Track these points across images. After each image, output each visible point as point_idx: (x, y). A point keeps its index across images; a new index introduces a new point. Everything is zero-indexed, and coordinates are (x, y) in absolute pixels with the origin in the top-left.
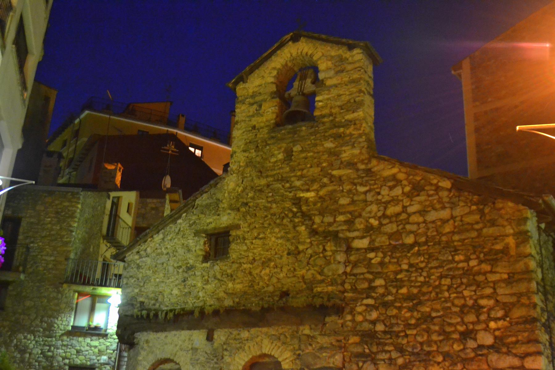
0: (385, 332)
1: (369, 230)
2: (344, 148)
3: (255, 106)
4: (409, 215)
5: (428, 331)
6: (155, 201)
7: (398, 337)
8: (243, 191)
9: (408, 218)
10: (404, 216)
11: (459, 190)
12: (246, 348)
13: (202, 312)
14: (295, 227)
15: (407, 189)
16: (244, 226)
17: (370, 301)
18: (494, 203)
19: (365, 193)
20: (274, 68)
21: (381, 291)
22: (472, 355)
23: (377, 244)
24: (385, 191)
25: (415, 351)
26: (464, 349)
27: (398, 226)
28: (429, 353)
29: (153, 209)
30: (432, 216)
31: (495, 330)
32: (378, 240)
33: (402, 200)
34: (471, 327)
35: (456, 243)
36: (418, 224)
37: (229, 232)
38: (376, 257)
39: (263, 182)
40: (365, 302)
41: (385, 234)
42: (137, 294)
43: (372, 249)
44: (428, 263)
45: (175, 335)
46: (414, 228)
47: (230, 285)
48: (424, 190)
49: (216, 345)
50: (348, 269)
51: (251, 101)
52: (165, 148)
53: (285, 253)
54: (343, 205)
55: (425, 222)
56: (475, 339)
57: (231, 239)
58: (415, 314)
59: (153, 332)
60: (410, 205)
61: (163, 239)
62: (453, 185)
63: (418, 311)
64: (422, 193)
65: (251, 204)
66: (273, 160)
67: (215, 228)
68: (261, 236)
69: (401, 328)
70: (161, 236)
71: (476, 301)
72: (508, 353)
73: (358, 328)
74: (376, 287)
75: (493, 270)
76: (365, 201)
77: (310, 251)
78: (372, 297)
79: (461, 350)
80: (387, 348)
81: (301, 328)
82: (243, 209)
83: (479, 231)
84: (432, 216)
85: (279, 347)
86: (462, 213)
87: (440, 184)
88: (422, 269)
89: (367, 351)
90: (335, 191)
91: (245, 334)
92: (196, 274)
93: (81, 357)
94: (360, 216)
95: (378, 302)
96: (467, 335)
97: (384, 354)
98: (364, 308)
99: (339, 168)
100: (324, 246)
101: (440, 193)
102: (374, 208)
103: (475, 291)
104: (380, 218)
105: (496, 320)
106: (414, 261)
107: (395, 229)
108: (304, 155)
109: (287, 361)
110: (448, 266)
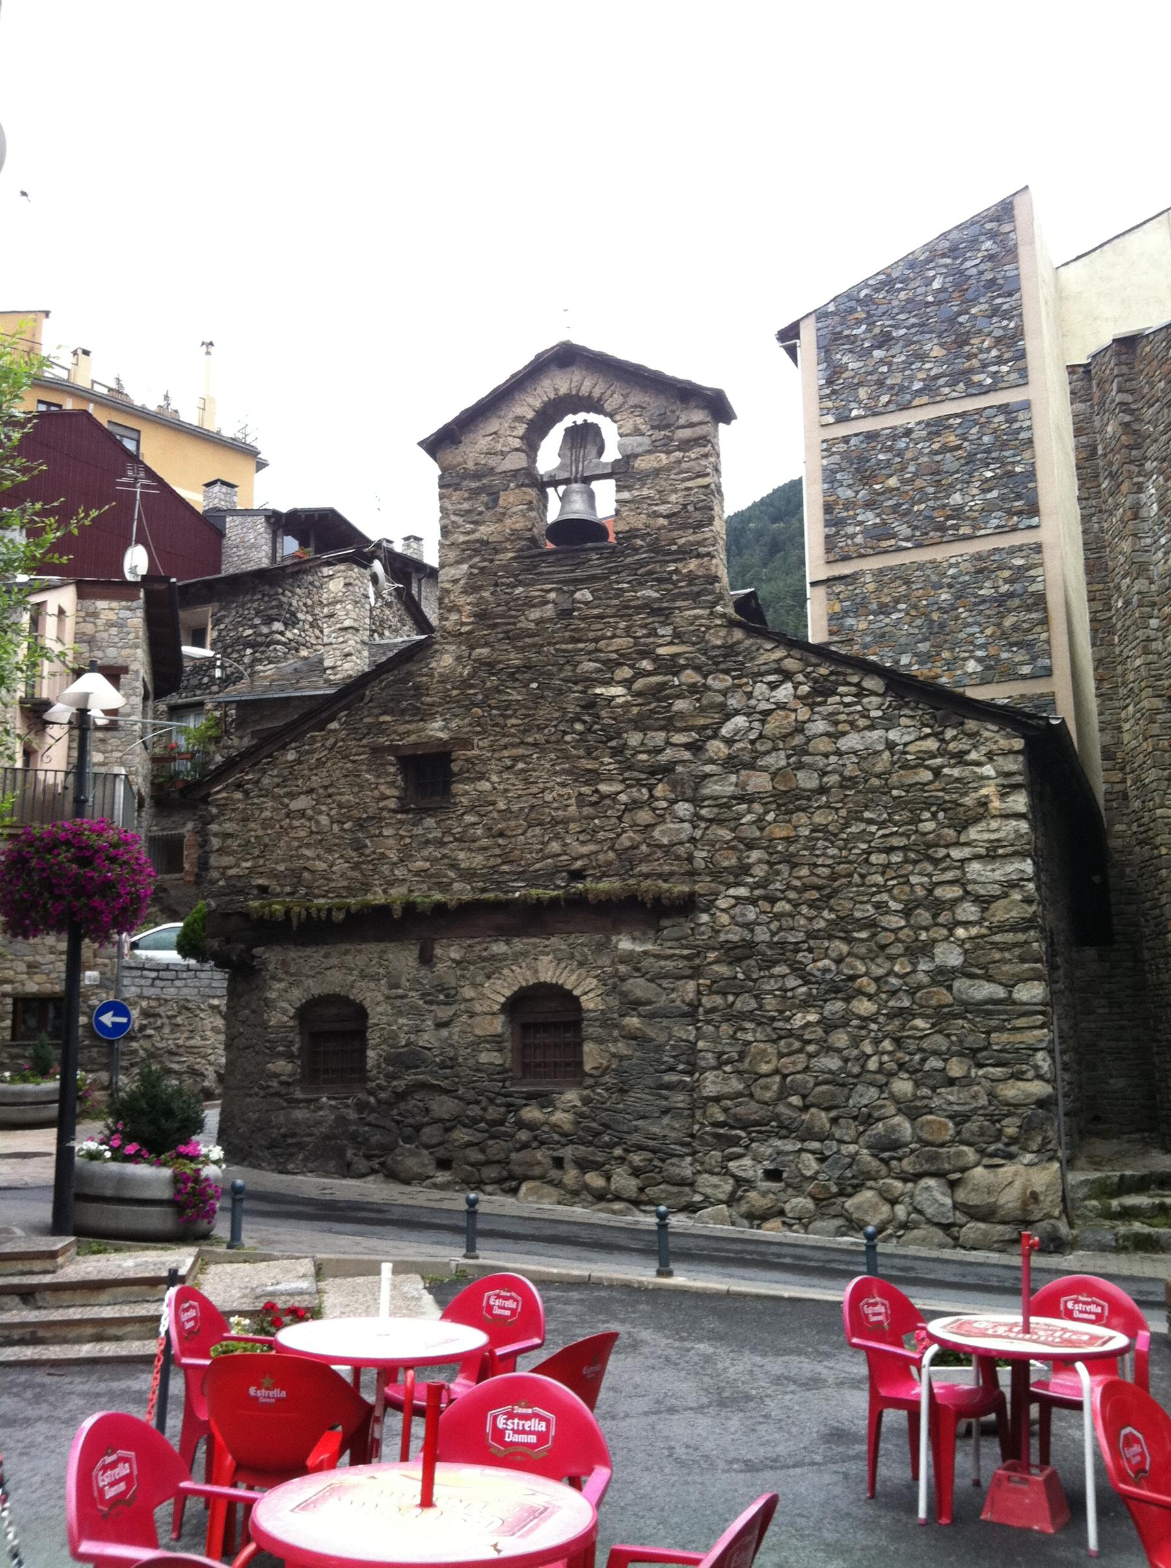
0: (771, 945)
1: (732, 764)
2: (678, 604)
3: (484, 498)
4: (809, 740)
5: (849, 940)
6: (114, 604)
7: (797, 951)
8: (472, 676)
9: (807, 743)
10: (798, 740)
11: (899, 696)
12: (506, 971)
13: (410, 908)
14: (589, 754)
15: (805, 689)
16: (481, 747)
17: (742, 891)
18: (962, 724)
19: (724, 693)
20: (519, 419)
21: (760, 871)
22: (926, 980)
23: (750, 789)
24: (760, 689)
25: (828, 976)
26: (914, 971)
27: (788, 757)
28: (852, 978)
29: (110, 624)
30: (851, 741)
31: (963, 941)
32: (752, 782)
33: (795, 710)
34: (923, 936)
35: (895, 793)
36: (826, 756)
37: (449, 754)
38: (749, 811)
39: (516, 659)
40: (732, 892)
41: (764, 769)
42: (251, 870)
43: (741, 799)
44: (847, 825)
45: (346, 953)
46: (821, 762)
47: (462, 855)
48: (834, 693)
49: (441, 967)
50: (698, 834)
51: (474, 485)
52: (124, 480)
53: (573, 801)
54: (681, 714)
55: (839, 753)
56: (933, 959)
57: (455, 767)
58: (825, 913)
59: (296, 945)
60: (809, 720)
61: (299, 762)
62: (888, 688)
63: (831, 910)
64: (830, 700)
65: (493, 702)
66: (535, 614)
67: (416, 745)
68: (521, 765)
69: (801, 936)
70: (291, 756)
71: (930, 892)
72: (989, 979)
73: (722, 937)
74: (750, 866)
75: (962, 840)
76: (723, 706)
77: (623, 797)
78: (745, 885)
79: (908, 974)
80: (778, 970)
81: (614, 939)
82: (477, 711)
83: (937, 772)
84: (851, 741)
85: (572, 971)
86: (907, 738)
87: (865, 684)
88: (835, 835)
89: (741, 976)
90: (663, 686)
91: (499, 948)
92: (385, 833)
93: (37, 978)
94: (715, 736)
95: (757, 892)
96: (918, 950)
97: (772, 981)
98: (733, 901)
99: (671, 643)
100: (650, 791)
101: (865, 700)
102: (740, 721)
103: (930, 876)
104: (753, 742)
105: (966, 924)
106: (819, 818)
107: (783, 763)
108: (595, 612)
109: (591, 995)
110: (881, 833)
